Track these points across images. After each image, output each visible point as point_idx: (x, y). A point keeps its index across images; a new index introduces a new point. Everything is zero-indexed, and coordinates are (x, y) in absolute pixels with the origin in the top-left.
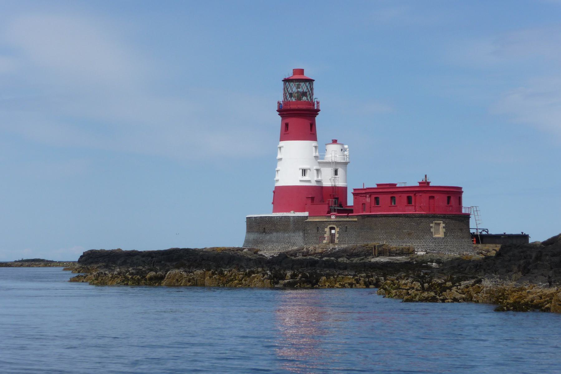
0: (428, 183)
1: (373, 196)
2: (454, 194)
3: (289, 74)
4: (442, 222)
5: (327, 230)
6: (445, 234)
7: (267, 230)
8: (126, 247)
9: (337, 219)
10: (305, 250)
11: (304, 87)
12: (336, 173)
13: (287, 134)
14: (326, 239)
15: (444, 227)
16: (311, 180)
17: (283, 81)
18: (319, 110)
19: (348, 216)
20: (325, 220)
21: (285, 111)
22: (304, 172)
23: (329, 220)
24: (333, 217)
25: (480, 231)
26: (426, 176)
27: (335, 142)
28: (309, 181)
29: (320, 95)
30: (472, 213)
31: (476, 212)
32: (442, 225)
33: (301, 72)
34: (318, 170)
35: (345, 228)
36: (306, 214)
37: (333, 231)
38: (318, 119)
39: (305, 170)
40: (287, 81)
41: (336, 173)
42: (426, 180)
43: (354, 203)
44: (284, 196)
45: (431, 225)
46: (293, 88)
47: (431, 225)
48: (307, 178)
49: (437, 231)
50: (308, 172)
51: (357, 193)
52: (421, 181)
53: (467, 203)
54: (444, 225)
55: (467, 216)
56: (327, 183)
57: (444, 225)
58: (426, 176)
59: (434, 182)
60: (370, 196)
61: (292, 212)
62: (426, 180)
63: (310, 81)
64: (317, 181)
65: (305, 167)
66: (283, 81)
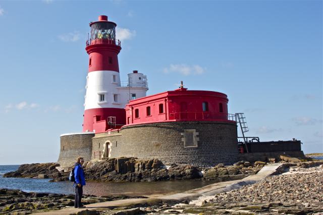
1: (135, 109)
2: (218, 101)
4: (195, 130)
5: (105, 145)
6: (199, 143)
7: (65, 148)
15: (197, 136)
19: (118, 132)
20: (104, 136)
22: (102, 97)
24: (109, 133)
25: (251, 139)
26: (182, 82)
29: (121, 36)
30: (238, 121)
31: (241, 120)
32: (195, 133)
33: (104, 18)
34: (115, 96)
39: (104, 96)
53: (232, 110)
54: (197, 134)
55: (233, 124)
57: (197, 134)
58: (182, 82)
60: (132, 108)
63: (112, 25)
65: (101, 92)
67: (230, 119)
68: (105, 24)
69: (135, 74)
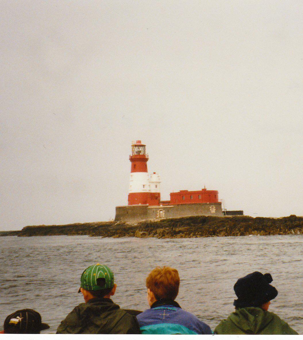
0: (206, 189)
3: (135, 143)
4: (214, 206)
6: (216, 211)
8: (82, 222)
9: (164, 207)
10: (149, 221)
11: (141, 149)
12: (156, 186)
13: (134, 169)
14: (158, 215)
16: (147, 190)
17: (132, 146)
18: (148, 159)
19: (168, 205)
21: (132, 159)
23: (159, 207)
26: (205, 186)
27: (154, 173)
28: (146, 190)
29: (149, 152)
33: (140, 142)
34: (149, 185)
35: (167, 210)
36: (148, 204)
37: (161, 212)
38: (148, 163)
40: (133, 146)
41: (156, 186)
42: (205, 188)
43: (171, 199)
44: (132, 197)
45: (210, 207)
46: (136, 149)
47: (210, 207)
48: (144, 189)
49: (212, 209)
50: (145, 187)
51: (172, 195)
52: (203, 189)
53: (221, 198)
55: (220, 204)
56: (153, 191)
58: (205, 186)
59: (208, 189)
61: (140, 204)
62: (205, 188)
63: (144, 146)
64: (149, 190)
65: (144, 184)
66: (132, 146)
67: (219, 201)
68: (139, 145)
69: (154, 174)
